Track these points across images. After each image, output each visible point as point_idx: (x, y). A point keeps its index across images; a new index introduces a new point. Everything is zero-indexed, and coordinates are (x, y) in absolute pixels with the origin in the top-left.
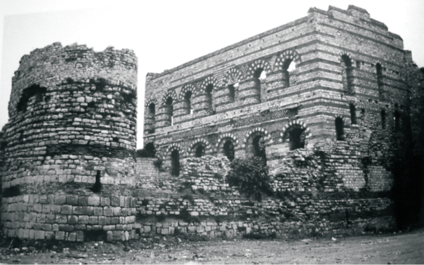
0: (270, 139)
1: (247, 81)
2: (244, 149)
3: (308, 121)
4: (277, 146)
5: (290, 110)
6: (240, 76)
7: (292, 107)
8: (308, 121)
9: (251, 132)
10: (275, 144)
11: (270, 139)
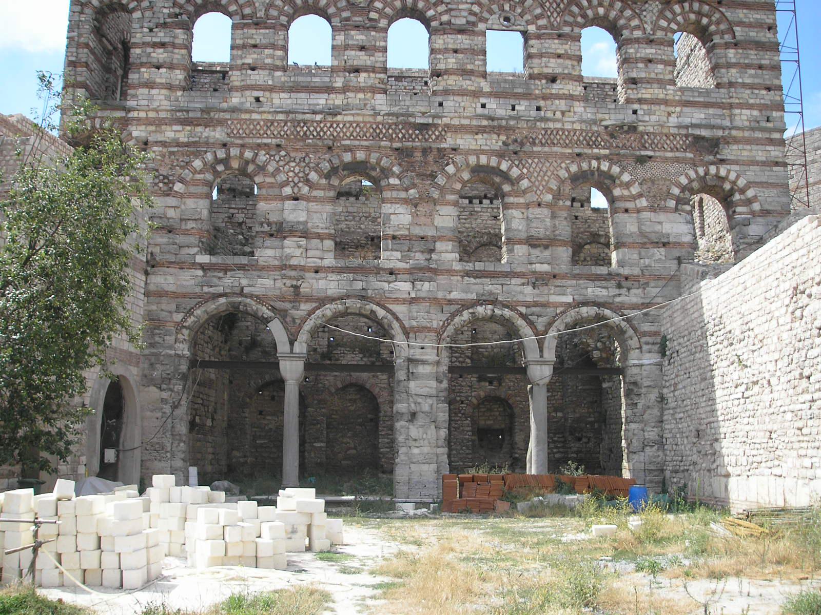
0: (640, 195)
1: (560, 36)
2: (549, 205)
3: (753, 173)
4: (662, 217)
5: (698, 139)
6: (538, 17)
7: (704, 133)
8: (753, 173)
9: (574, 168)
10: (652, 209)
11: (640, 195)
